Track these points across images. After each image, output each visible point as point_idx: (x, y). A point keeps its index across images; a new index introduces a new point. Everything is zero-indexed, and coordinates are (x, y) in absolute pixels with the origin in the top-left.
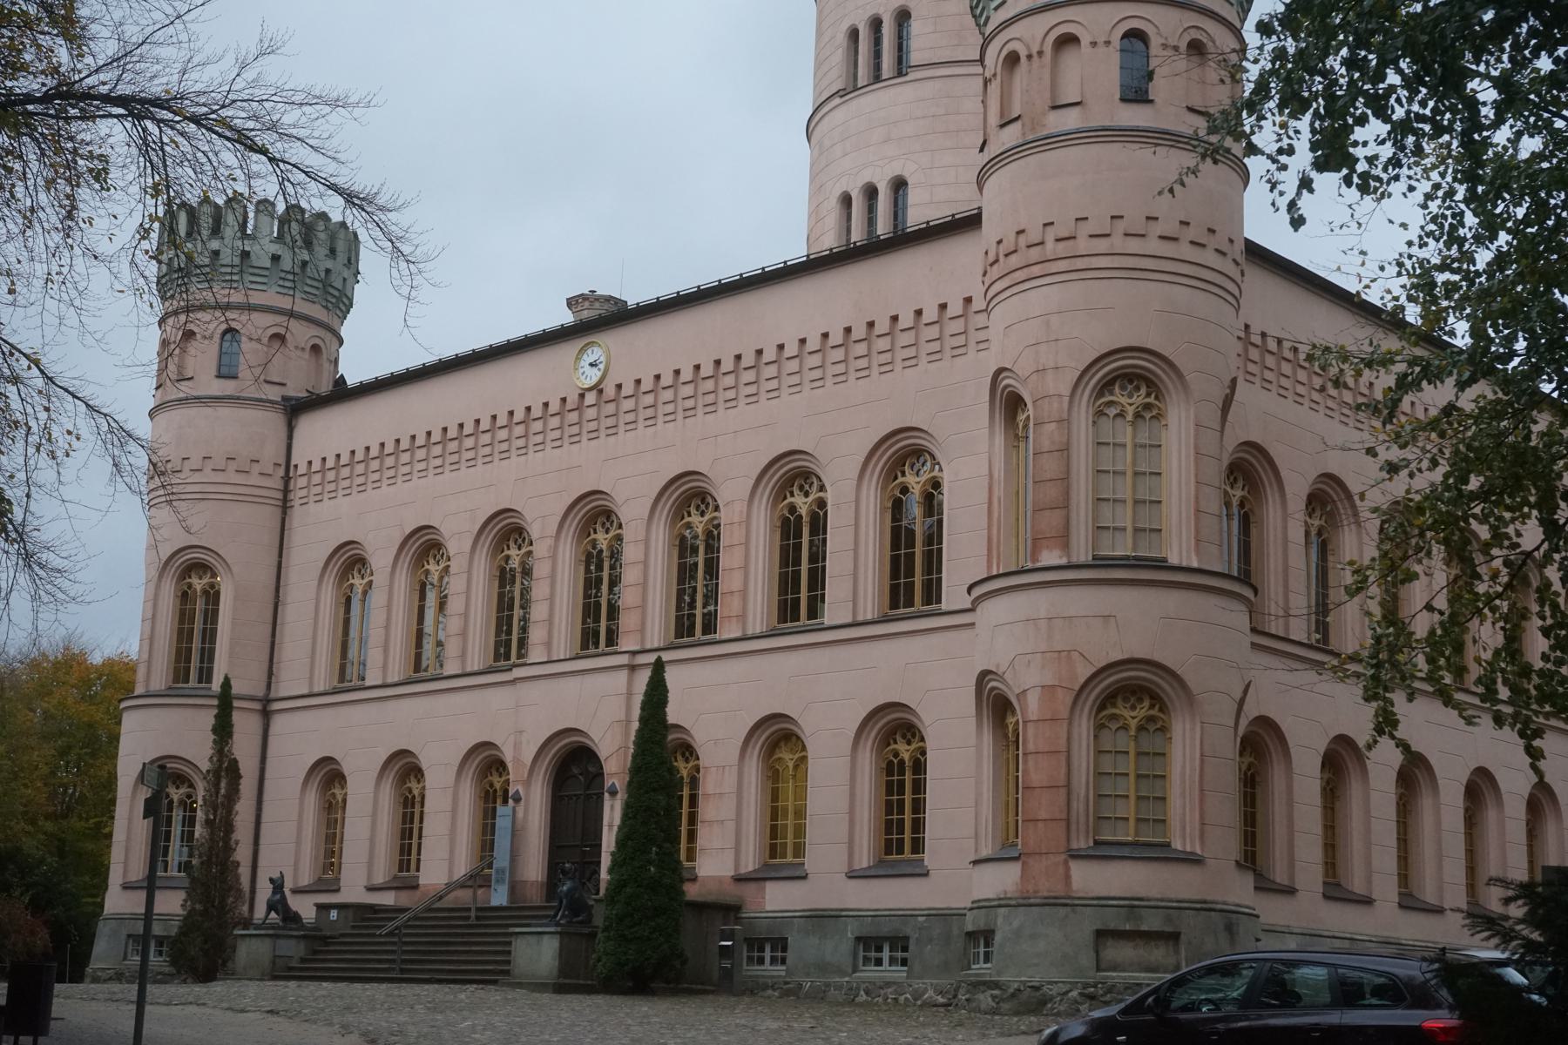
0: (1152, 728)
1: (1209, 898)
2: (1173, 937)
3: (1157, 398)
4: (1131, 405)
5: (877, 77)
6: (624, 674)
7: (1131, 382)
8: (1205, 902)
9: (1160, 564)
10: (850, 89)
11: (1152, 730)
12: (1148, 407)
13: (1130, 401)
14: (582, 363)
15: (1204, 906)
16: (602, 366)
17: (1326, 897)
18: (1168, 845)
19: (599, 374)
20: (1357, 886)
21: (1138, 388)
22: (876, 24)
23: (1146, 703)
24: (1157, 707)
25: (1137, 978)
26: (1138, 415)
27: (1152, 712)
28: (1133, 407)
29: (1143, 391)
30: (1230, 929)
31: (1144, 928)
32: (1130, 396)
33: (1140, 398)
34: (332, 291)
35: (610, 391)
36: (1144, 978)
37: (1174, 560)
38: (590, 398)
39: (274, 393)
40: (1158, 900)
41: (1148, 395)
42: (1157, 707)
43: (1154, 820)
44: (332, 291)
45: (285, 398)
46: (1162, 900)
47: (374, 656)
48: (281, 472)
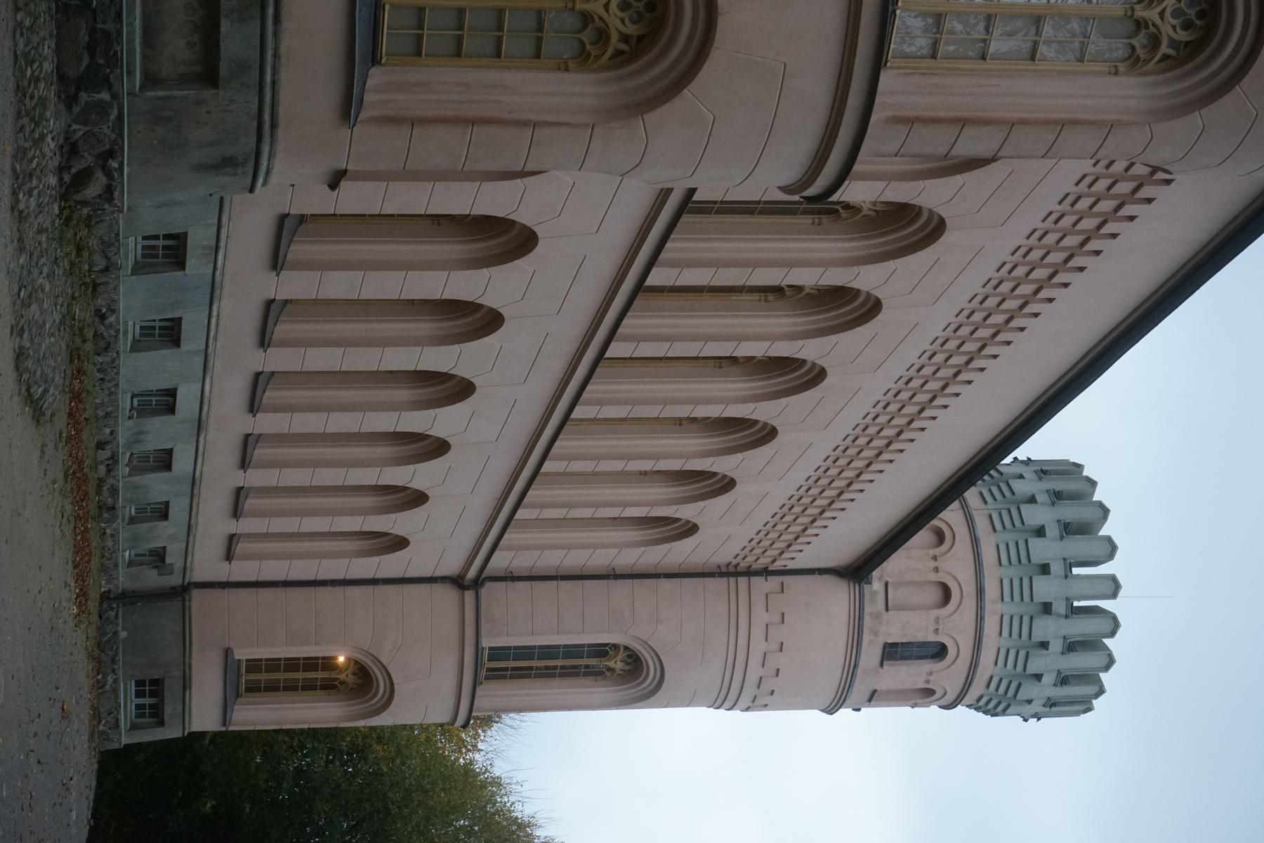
0: (586, 36)
1: (281, 133)
2: (209, 76)
3: (1166, 57)
4: (1162, 14)
7: (1202, 15)
8: (274, 126)
9: (878, 62)
11: (581, 36)
12: (1155, 41)
13: (1168, 13)
15: (267, 126)
17: (283, 218)
18: (375, 60)
20: (298, 250)
21: (1187, 26)
23: (631, 29)
24: (623, 47)
25: (131, 12)
26: (1140, 24)
27: (614, 37)
28: (1158, 21)
29: (1182, 36)
30: (228, 164)
31: (225, 26)
32: (1177, 13)
33: (1170, 30)
36: (131, 24)
37: (886, 79)
40: (276, 49)
41: (1173, 43)
42: (623, 47)
43: (420, 37)
46: (276, 55)
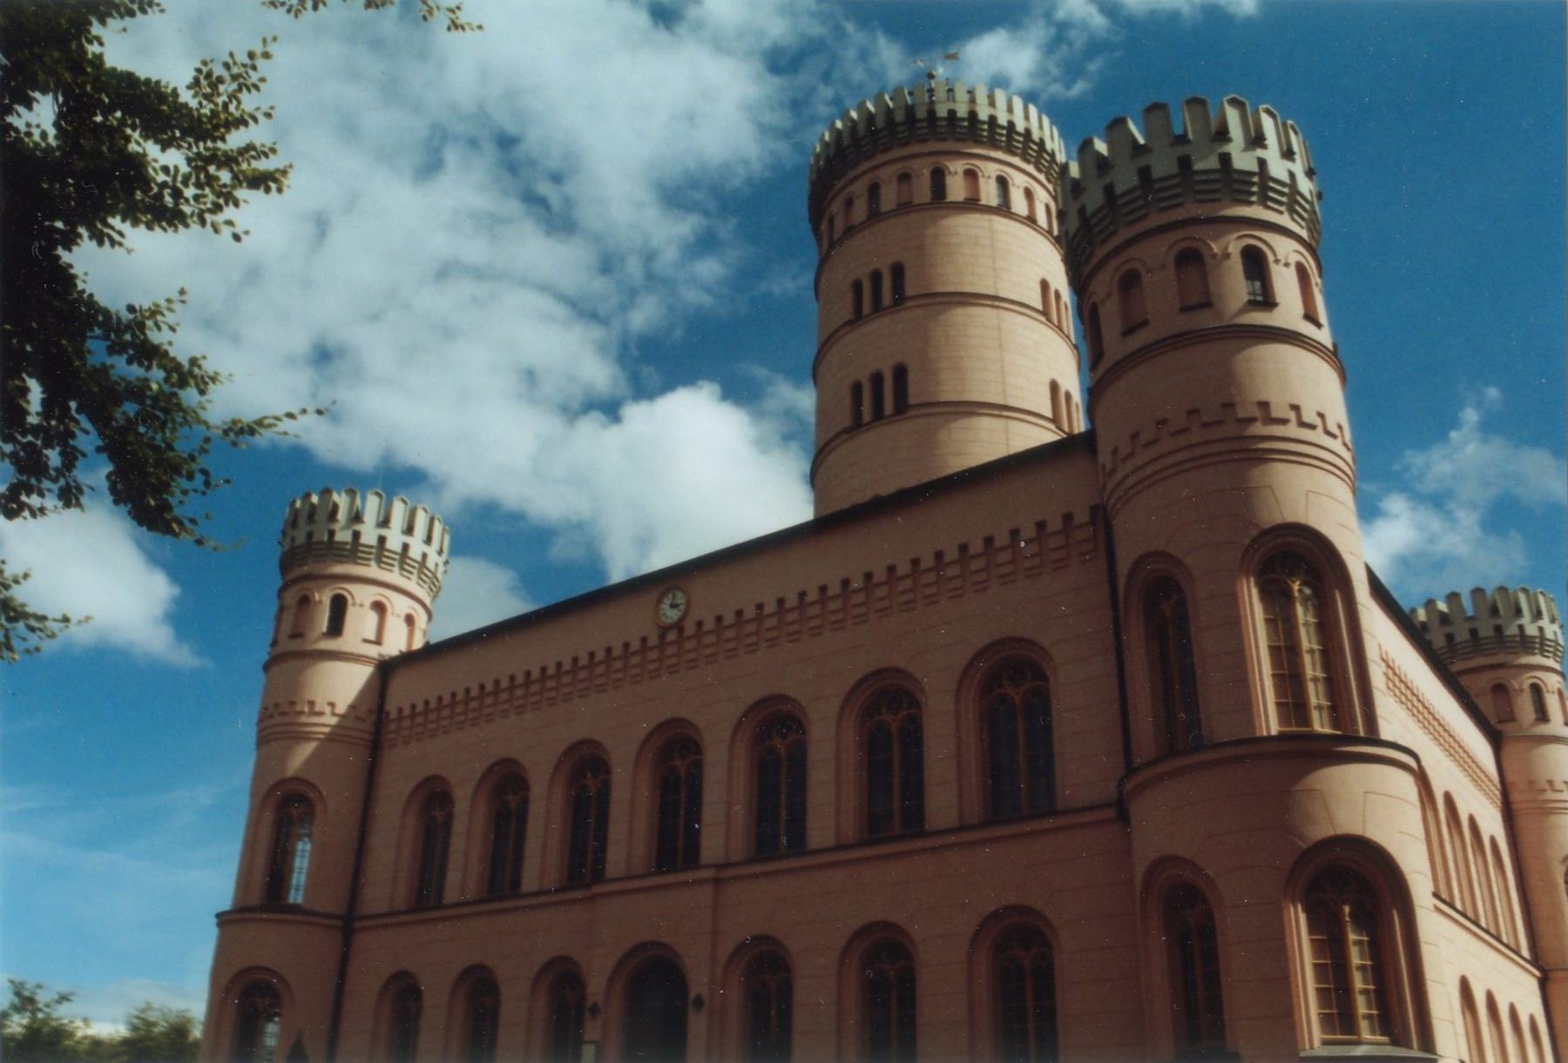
5: (878, 414)
6: (708, 890)
10: (857, 425)
14: (663, 606)
16: (682, 607)
19: (679, 614)
22: (877, 379)
34: (426, 571)
35: (690, 629)
38: (671, 636)
39: (373, 651)
44: (426, 571)
45: (380, 655)
47: (453, 878)
48: (374, 717)
